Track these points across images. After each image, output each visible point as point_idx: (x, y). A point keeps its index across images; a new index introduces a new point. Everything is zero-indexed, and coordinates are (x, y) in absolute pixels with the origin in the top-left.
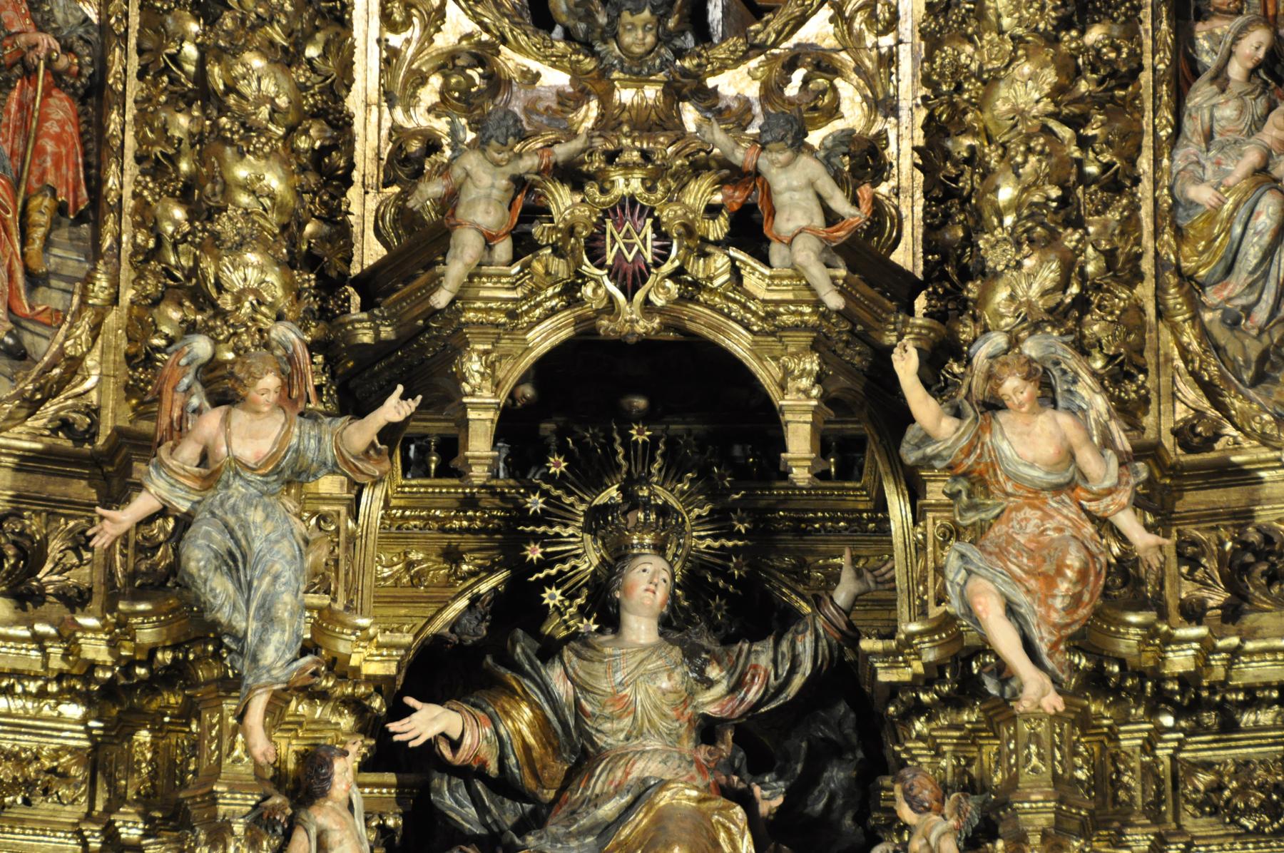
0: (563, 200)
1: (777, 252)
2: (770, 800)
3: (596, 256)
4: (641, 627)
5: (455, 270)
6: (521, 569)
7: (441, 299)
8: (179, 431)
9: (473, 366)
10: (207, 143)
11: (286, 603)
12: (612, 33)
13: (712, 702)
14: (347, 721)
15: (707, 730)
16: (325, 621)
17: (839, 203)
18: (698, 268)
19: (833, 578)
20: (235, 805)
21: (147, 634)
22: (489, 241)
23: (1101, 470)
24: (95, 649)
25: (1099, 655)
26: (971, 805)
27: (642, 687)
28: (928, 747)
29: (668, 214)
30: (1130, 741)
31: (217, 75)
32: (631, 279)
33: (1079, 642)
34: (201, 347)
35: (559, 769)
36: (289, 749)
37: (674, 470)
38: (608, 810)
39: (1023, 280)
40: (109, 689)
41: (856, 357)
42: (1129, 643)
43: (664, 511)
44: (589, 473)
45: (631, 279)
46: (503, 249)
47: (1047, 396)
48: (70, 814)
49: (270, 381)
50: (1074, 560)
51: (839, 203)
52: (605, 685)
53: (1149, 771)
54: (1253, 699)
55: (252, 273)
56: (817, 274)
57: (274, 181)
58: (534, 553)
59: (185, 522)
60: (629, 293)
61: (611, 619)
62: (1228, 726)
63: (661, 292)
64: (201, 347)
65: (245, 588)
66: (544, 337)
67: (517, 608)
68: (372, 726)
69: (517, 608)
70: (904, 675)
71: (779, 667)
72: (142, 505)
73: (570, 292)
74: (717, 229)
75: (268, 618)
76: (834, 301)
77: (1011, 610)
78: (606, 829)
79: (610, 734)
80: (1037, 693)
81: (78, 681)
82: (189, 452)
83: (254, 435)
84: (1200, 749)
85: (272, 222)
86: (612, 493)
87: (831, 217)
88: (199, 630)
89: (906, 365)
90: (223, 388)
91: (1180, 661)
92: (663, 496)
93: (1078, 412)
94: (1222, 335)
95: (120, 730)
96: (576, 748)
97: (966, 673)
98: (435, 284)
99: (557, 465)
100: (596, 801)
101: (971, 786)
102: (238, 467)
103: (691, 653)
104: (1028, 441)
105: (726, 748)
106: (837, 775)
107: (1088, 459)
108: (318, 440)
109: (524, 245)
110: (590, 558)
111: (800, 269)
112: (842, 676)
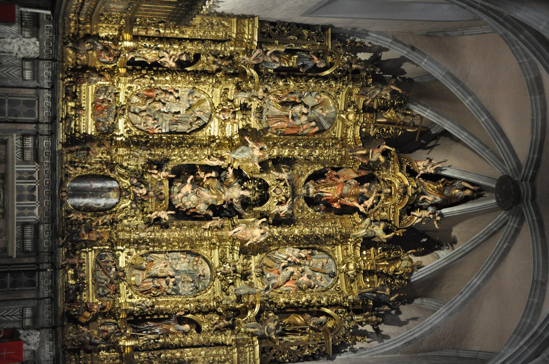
0: (282, 184)
1: (277, 206)
2: (225, 206)
3: (277, 187)
4: (242, 193)
5: (274, 173)
6: (249, 180)
7: (272, 172)
8: (257, 145)
9: (265, 175)
10: (290, 147)
11: (238, 156)
12: (304, 189)
13: (234, 200)
14: (229, 162)
15: (232, 200)
16: (238, 160)
17: (283, 213)
18: (275, 198)
19: (250, 213)
20: (219, 152)
21: (236, 142)
22: (278, 176)
23: (255, 240)
24: (235, 137)
25: (235, 240)
26: (220, 227)
27: (235, 193)
28: (227, 222)
29: (281, 195)
30: (228, 243)
31: (297, 148)
32: (274, 191)
33: (237, 238)
34: (266, 147)
35: (227, 184)
36: (226, 157)
37: (260, 196)
38: (222, 190)
39: (275, 231)
40: (232, 139)
41: (268, 215)
42: (237, 243)
43: (255, 195)
44: (259, 187)
45: (274, 191)
46: (277, 178)
47: (262, 234)
48: (219, 135)
49: (261, 154)
50: (244, 237)
51: (283, 213)
52: (236, 189)
53: (225, 245)
54: (233, 255)
55: (275, 152)
56: (275, 211)
57: (286, 154)
58: (250, 181)
59: (247, 146)
60: (274, 191)
61: (243, 189)
62: (230, 253)
63: (274, 194)
64: (266, 147)
65: (240, 152)
66: (268, 182)
67: (246, 179)
68: (229, 165)
69: (246, 179)
70: (234, 220)
71: (238, 207)
72: (249, 142)
73: (273, 185)
74: (280, 200)
75: (237, 155)
76: (272, 212)
77: (239, 230)
78: (220, 189)
79: (231, 189)
80: (231, 233)
81: (233, 135)
82: (255, 146)
83: (257, 153)
84: (228, 250)
85: (281, 154)
86: (257, 189)
87: (281, 212)
88: (237, 147)
89: (264, 220)
90: (261, 149)
91: (236, 248)
92: (257, 195)
93: (260, 237)
94: (272, 252)
95: (228, 140)
96: (229, 186)
97: (234, 226)
98: (273, 171)
99: (260, 183)
100: (223, 188)
101: (223, 227)
102: (253, 151)
103: (239, 198)
104: (257, 232)
105: (230, 202)
106: (228, 213)
107: (256, 238)
108: (256, 159)
109: (277, 180)
110: (250, 187)
111: (275, 209)
112: (237, 213)
